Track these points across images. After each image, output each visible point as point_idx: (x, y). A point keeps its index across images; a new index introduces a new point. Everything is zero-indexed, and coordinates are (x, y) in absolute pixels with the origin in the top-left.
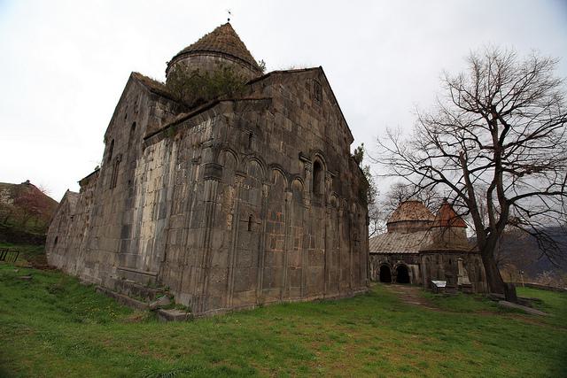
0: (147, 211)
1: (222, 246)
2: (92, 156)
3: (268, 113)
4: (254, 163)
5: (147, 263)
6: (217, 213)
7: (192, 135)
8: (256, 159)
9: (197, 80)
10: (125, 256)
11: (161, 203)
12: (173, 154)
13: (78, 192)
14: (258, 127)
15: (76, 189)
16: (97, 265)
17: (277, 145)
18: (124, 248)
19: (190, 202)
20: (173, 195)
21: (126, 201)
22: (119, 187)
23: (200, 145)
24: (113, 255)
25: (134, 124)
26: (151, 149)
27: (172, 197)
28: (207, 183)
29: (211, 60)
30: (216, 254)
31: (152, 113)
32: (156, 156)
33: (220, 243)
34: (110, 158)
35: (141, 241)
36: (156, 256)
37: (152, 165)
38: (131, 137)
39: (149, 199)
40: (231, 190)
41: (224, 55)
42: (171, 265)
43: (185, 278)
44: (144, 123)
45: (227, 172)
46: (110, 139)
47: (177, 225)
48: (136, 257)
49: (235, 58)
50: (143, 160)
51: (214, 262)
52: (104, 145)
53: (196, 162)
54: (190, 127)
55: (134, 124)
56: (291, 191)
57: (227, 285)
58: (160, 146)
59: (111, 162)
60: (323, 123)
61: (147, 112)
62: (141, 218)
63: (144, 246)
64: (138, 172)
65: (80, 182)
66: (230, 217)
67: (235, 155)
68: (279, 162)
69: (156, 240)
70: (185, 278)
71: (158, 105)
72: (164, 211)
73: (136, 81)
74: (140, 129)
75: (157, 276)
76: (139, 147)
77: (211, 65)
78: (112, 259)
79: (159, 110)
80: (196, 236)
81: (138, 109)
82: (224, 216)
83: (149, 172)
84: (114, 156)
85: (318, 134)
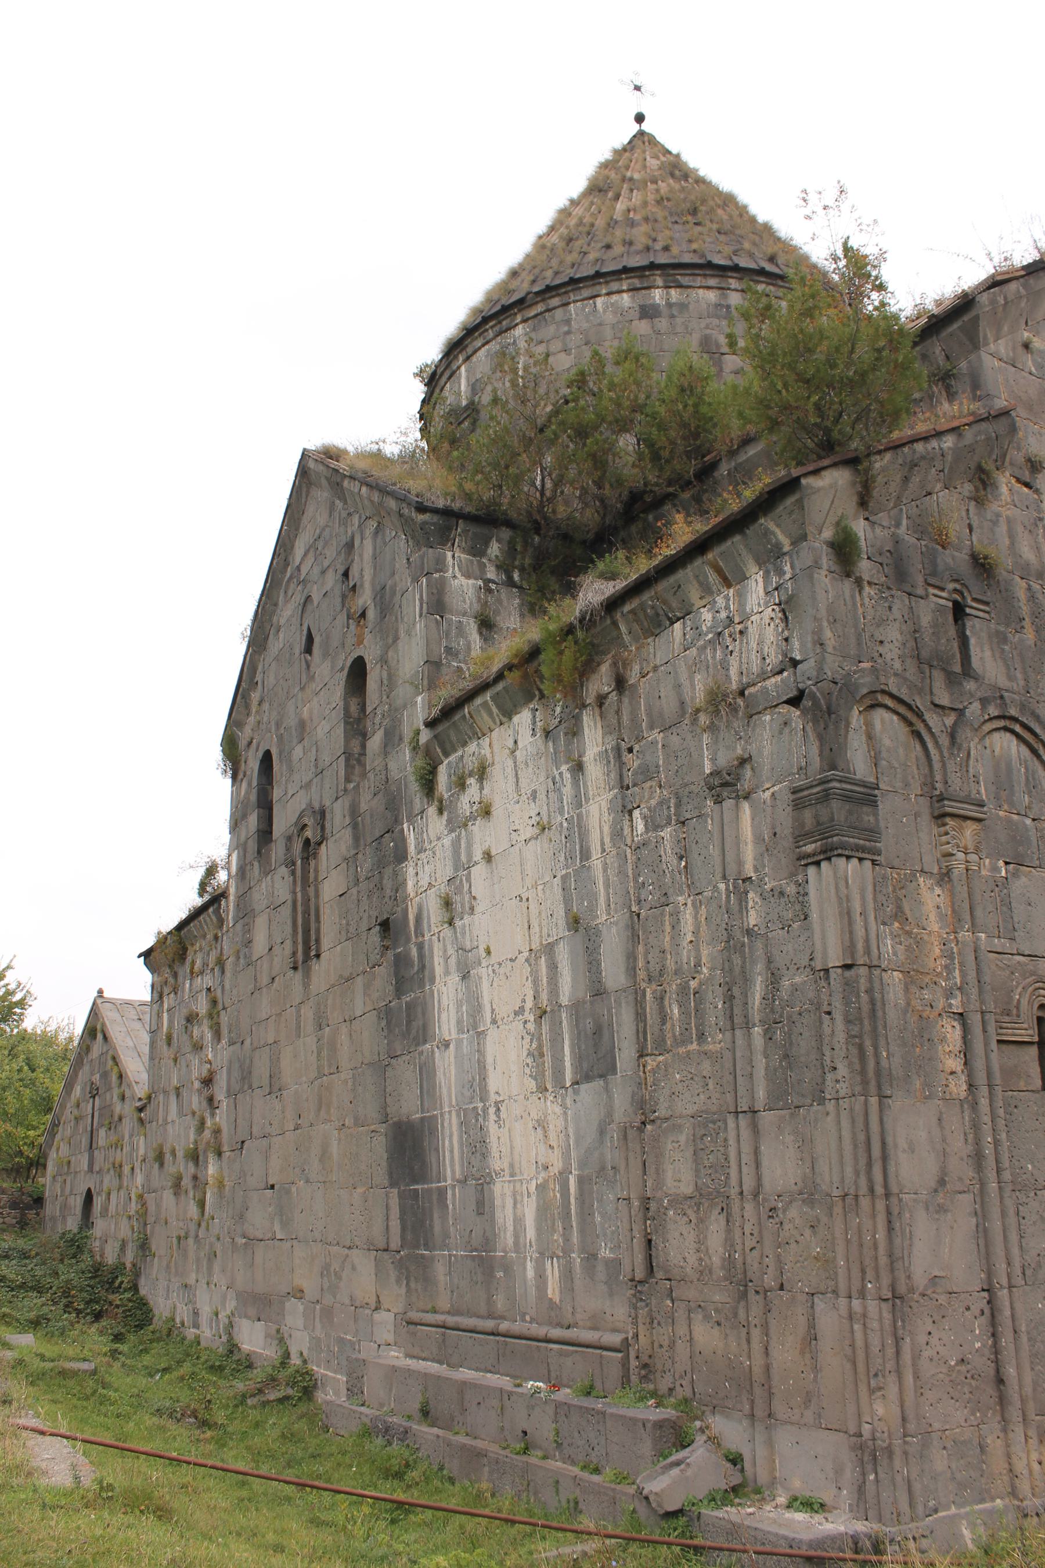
0: (507, 1056)
1: (942, 1182)
2: (183, 829)
3: (1005, 483)
4: (1005, 744)
5: (553, 1290)
6: (892, 1015)
7: (674, 663)
8: (1008, 723)
9: (576, 423)
10: (424, 1265)
11: (576, 1007)
12: (595, 771)
13: (147, 997)
14: (982, 566)
15: (136, 984)
16: (295, 1310)
18: (417, 1223)
20: (631, 957)
21: (387, 1014)
22: (335, 956)
23: (730, 704)
24: (364, 1264)
25: (358, 671)
26: (471, 763)
27: (632, 970)
28: (820, 881)
29: (617, 309)
30: (921, 1227)
32: (499, 787)
33: (931, 1167)
34: (265, 834)
35: (501, 1190)
36: (591, 1258)
37: (484, 836)
38: (356, 726)
39: (506, 991)
41: (673, 271)
42: (690, 1293)
43: (786, 1353)
44: (411, 655)
45: (900, 815)
46: (251, 756)
47: (684, 1097)
48: (486, 1262)
49: (722, 271)
51: (921, 1265)
52: (226, 784)
53: (726, 785)
54: (656, 624)
55: (358, 671)
57: (1000, 1381)
58: (512, 747)
59: (277, 850)
63: (517, 1213)
64: (424, 878)
65: (147, 955)
66: (953, 1033)
67: (910, 715)
69: (581, 1181)
70: (786, 1353)
71: (455, 558)
72: (588, 1044)
73: (320, 476)
74: (390, 684)
75: (624, 1347)
76: (404, 764)
78: (363, 1277)
79: (463, 590)
80: (805, 1143)
81: (365, 598)
82: (924, 1034)
83: (479, 872)
84: (282, 824)
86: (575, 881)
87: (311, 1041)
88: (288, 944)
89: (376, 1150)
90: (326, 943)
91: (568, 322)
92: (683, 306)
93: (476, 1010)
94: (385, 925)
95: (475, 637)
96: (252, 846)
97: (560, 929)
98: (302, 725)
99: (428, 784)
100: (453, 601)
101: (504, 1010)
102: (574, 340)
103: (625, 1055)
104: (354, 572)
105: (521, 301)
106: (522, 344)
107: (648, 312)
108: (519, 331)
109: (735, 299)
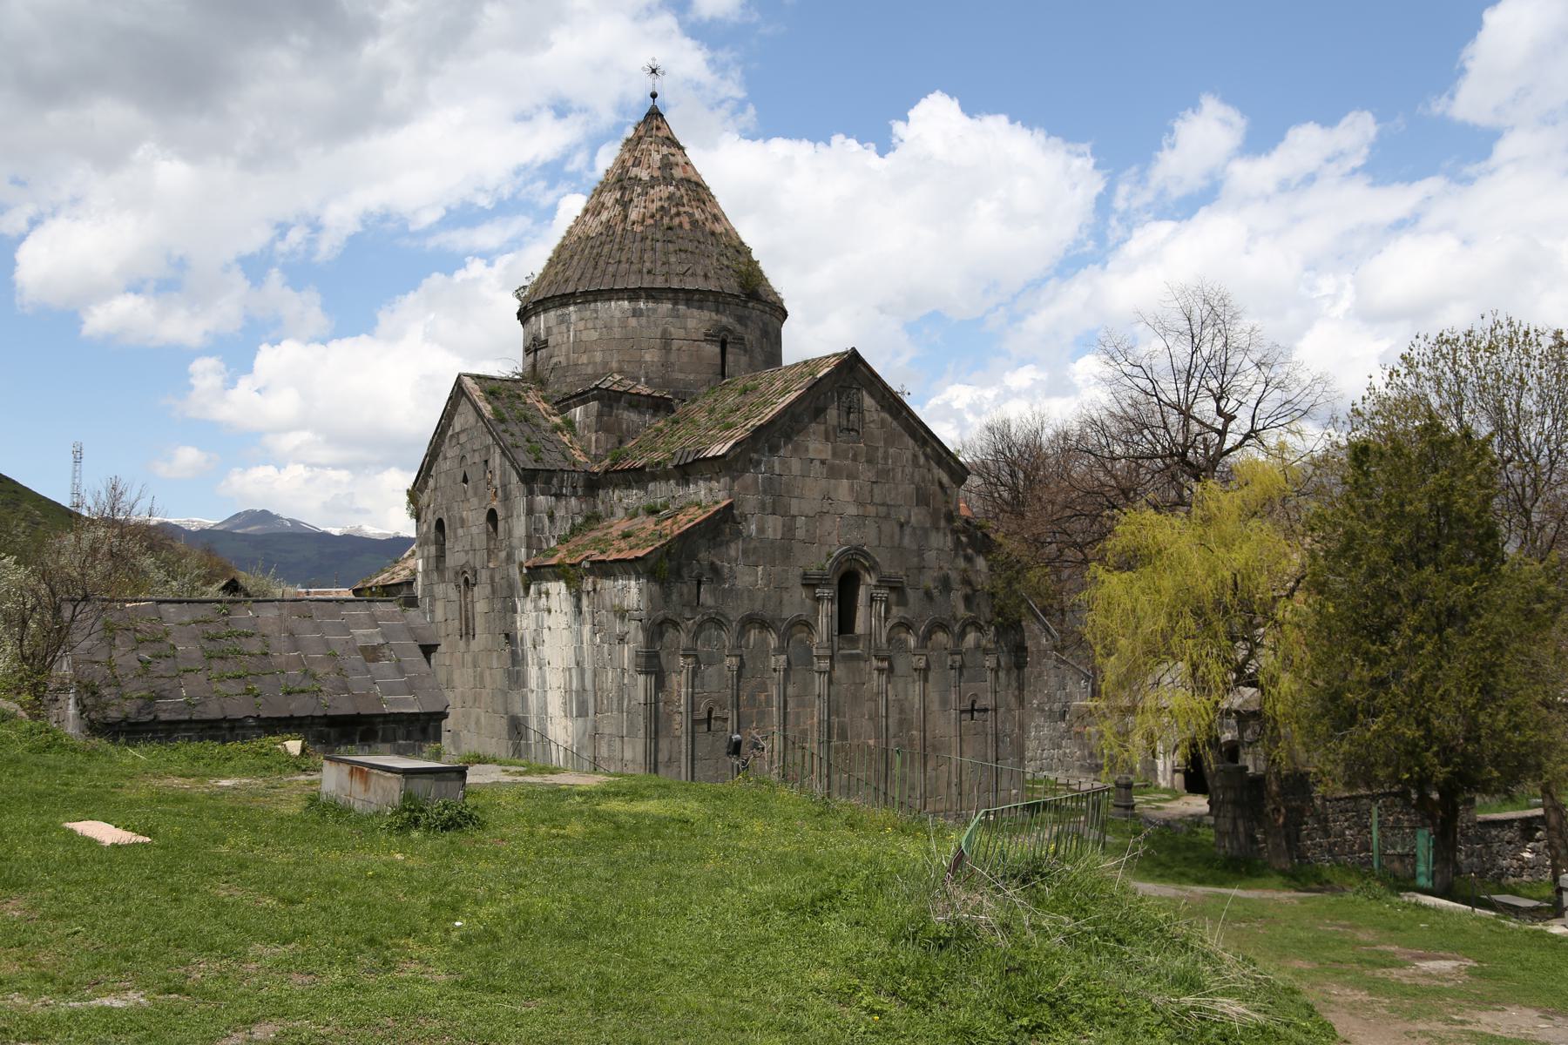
17: (749, 578)
19: (621, 700)
21: (509, 674)
22: (481, 639)
31: (530, 511)
37: (549, 621)
39: (555, 679)
40: (674, 678)
47: (607, 729)
50: (529, 605)
56: (780, 650)
59: (449, 575)
60: (866, 473)
61: (520, 504)
62: (544, 708)
64: (525, 623)
68: (758, 606)
72: (581, 704)
77: (623, 325)
83: (546, 631)
85: (852, 510)
86: (579, 649)
87: (470, 671)
88: (457, 622)
89: (502, 725)
90: (478, 631)
91: (596, 311)
92: (655, 310)
93: (544, 682)
94: (507, 636)
95: (546, 521)
96: (432, 562)
97: (573, 665)
98: (462, 521)
99: (527, 589)
100: (537, 507)
101: (555, 686)
102: (600, 323)
103: (591, 712)
104: (491, 463)
105: (573, 294)
106: (574, 317)
107: (636, 313)
108: (571, 308)
109: (682, 308)
